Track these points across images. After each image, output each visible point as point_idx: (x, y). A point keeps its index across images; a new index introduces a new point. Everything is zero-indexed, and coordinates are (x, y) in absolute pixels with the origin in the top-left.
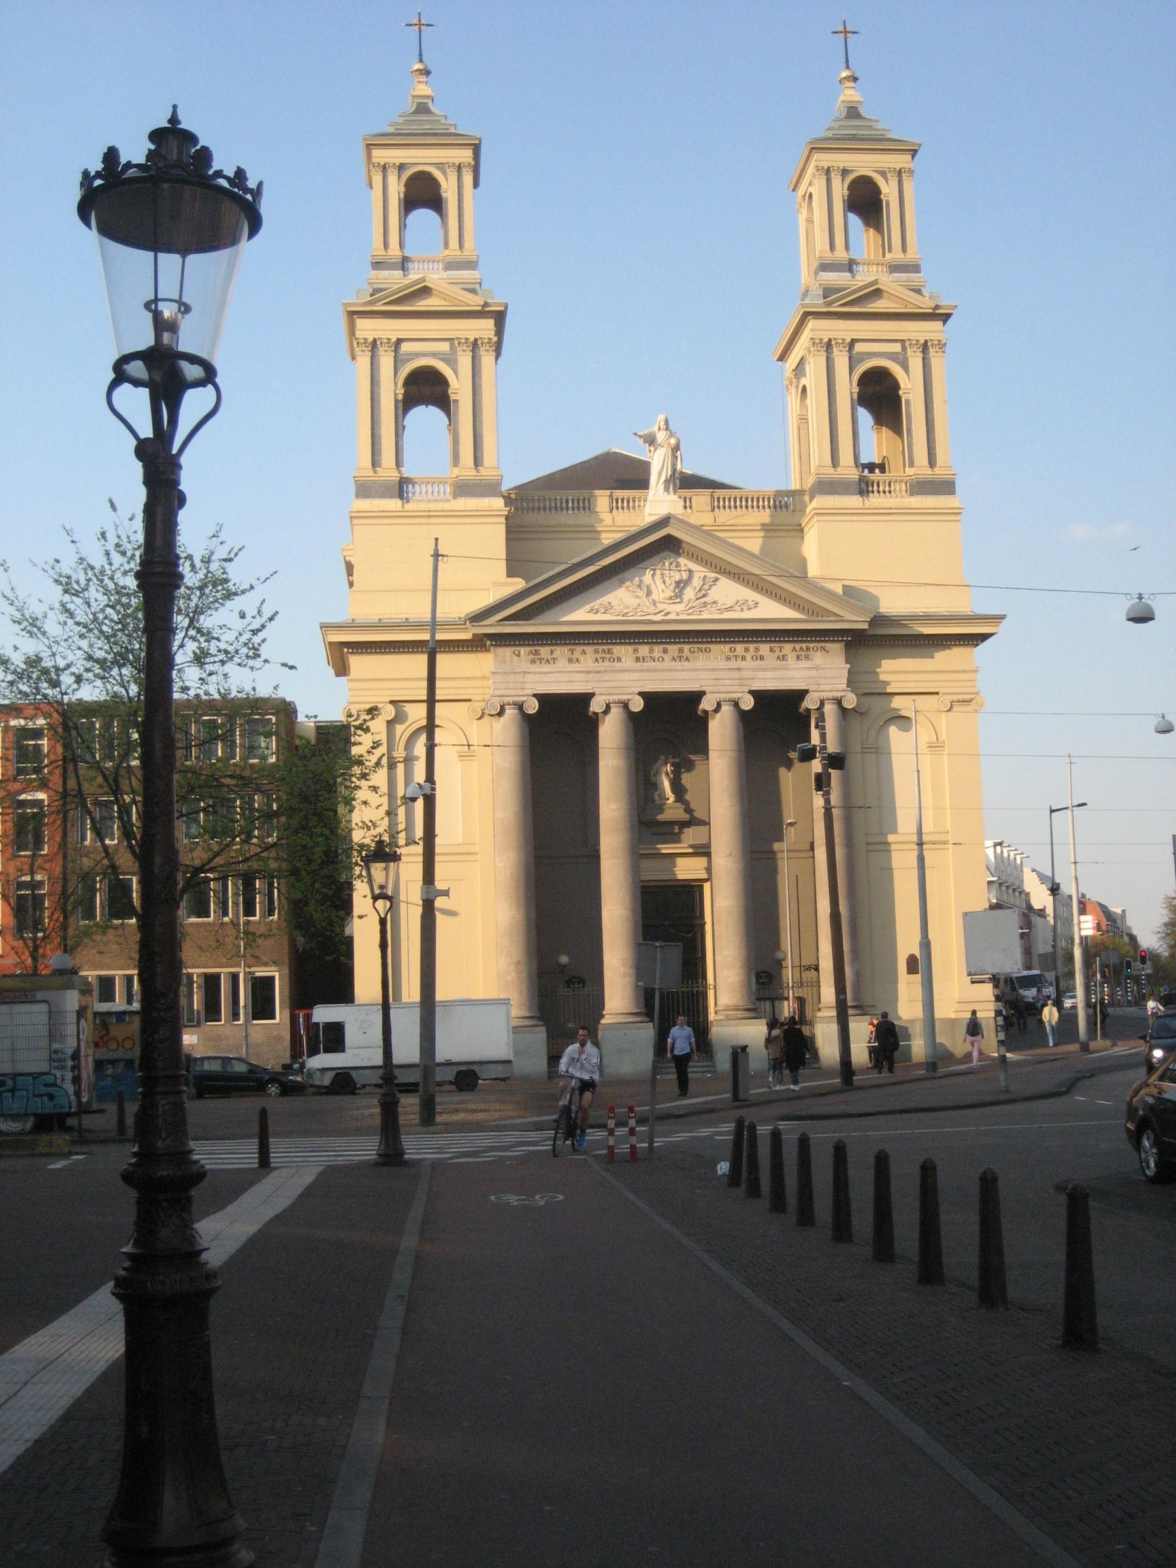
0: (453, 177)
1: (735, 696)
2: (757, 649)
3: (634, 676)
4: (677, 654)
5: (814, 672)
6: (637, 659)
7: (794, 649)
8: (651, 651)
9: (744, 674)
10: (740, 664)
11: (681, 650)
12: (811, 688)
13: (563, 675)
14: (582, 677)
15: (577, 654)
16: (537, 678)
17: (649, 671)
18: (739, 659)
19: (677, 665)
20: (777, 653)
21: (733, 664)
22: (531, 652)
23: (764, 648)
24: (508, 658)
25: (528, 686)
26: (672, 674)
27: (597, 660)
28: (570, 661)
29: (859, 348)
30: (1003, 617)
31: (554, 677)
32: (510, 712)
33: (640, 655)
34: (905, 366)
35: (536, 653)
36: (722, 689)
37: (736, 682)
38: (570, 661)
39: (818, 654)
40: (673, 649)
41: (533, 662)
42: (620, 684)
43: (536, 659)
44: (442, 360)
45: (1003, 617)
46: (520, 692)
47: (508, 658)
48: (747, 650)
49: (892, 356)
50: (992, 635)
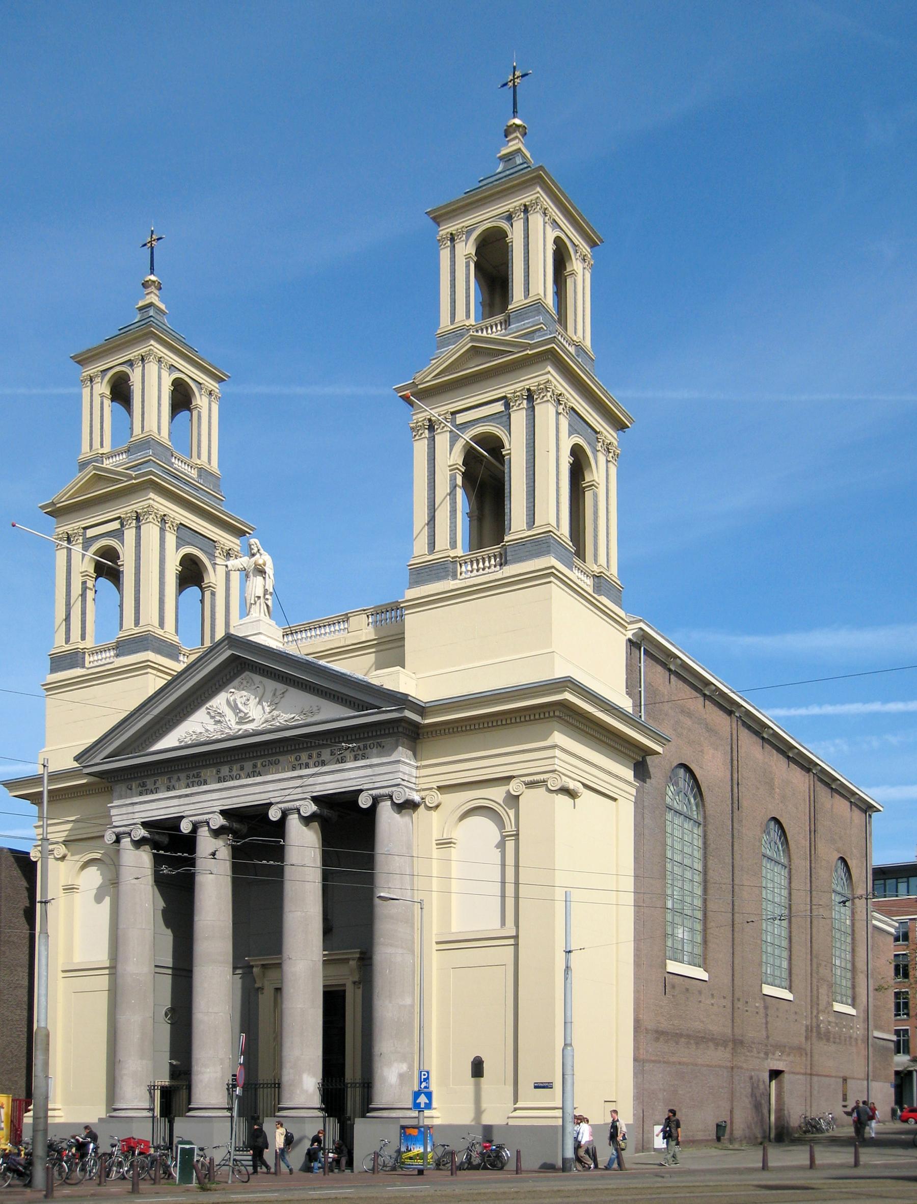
1: (297, 804)
15: (173, 782)
33: (221, 775)
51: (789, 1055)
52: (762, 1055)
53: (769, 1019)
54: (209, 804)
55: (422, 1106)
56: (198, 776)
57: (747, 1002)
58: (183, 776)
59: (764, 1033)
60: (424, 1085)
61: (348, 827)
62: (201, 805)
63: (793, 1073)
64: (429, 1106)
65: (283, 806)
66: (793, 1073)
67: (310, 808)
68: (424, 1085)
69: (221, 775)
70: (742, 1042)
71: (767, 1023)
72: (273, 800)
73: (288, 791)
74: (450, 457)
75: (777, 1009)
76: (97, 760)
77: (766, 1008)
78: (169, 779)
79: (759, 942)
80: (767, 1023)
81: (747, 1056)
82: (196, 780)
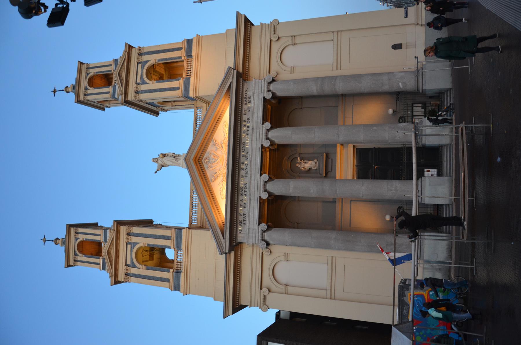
0: (80, 236)
3: (253, 178)
4: (244, 158)
5: (256, 95)
6: (246, 176)
7: (245, 104)
8: (243, 169)
9: (255, 127)
10: (250, 129)
11: (243, 155)
12: (262, 96)
13: (251, 211)
14: (252, 202)
15: (242, 204)
16: (251, 223)
17: (251, 171)
18: (249, 129)
19: (249, 157)
20: (247, 112)
21: (250, 132)
22: (240, 225)
23: (245, 117)
24: (242, 236)
26: (252, 159)
27: (245, 195)
28: (245, 207)
30: (238, 12)
31: (252, 215)
32: (266, 236)
33: (244, 175)
34: (147, 61)
35: (241, 222)
36: (261, 137)
37: (258, 130)
38: (245, 207)
39: (248, 93)
40: (243, 159)
41: (244, 224)
42: (256, 184)
43: (243, 223)
44: (133, 248)
45: (238, 12)
46: (257, 231)
47: (242, 236)
48: (245, 126)
49: (143, 67)
50: (245, 17)
54: (256, 181)
58: (241, 198)
61: (279, 110)
65: (263, 140)
67: (268, 125)
76: (224, 245)
78: (241, 206)
82: (244, 189)
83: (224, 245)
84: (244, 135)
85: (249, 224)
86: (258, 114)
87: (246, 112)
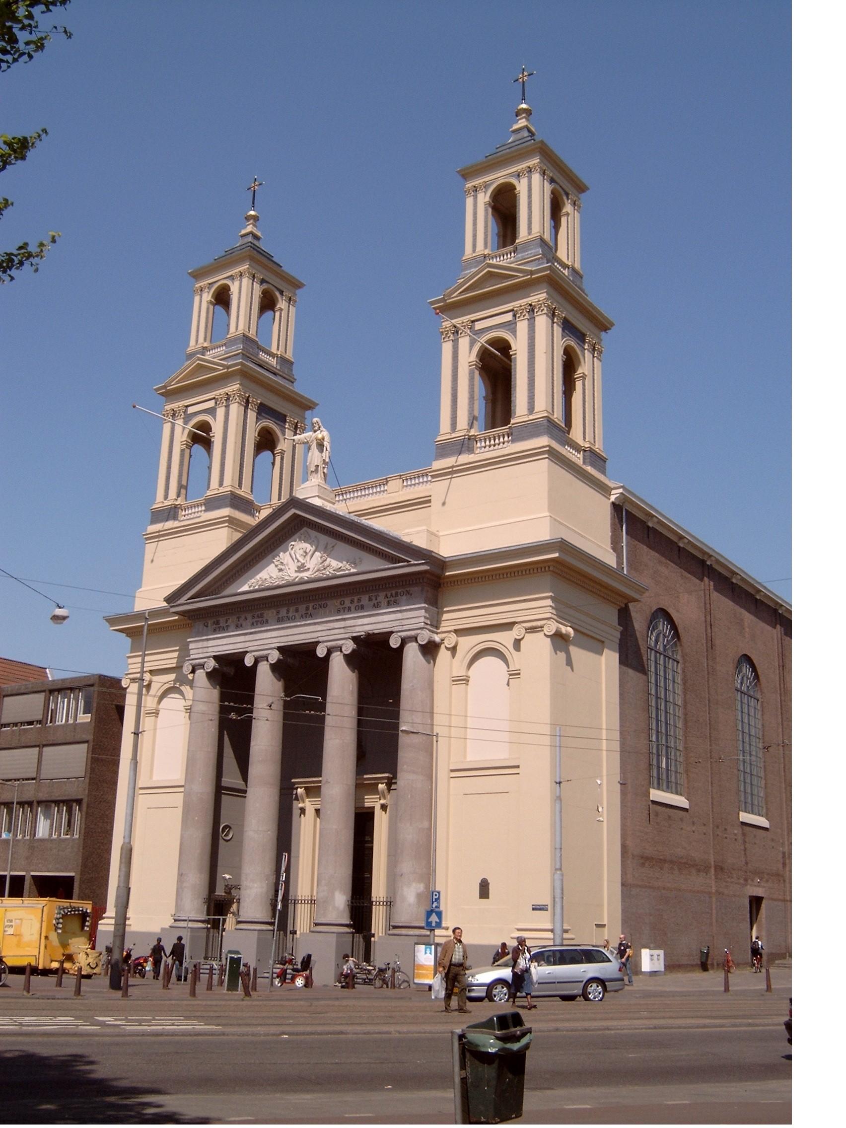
2: (359, 600)
7: (386, 596)
8: (288, 611)
14: (242, 638)
15: (241, 621)
23: (365, 600)
25: (210, 649)
29: (479, 326)
33: (280, 616)
37: (342, 631)
39: (404, 597)
40: (302, 608)
48: (352, 601)
51: (767, 881)
52: (742, 881)
53: (747, 845)
55: (434, 924)
56: (261, 616)
57: (726, 829)
58: (249, 616)
59: (743, 859)
60: (435, 904)
62: (261, 643)
63: (772, 899)
64: (439, 925)
66: (772, 899)
68: (435, 904)
69: (280, 616)
70: (722, 869)
71: (745, 850)
72: (320, 639)
73: (333, 633)
74: (468, 356)
75: (755, 836)
77: (744, 834)
78: (238, 618)
79: (735, 771)
80: (745, 850)
81: (727, 882)
83: (179, 602)
84: (336, 602)
85: (214, 639)
86: (368, 623)
87: (374, 598)
